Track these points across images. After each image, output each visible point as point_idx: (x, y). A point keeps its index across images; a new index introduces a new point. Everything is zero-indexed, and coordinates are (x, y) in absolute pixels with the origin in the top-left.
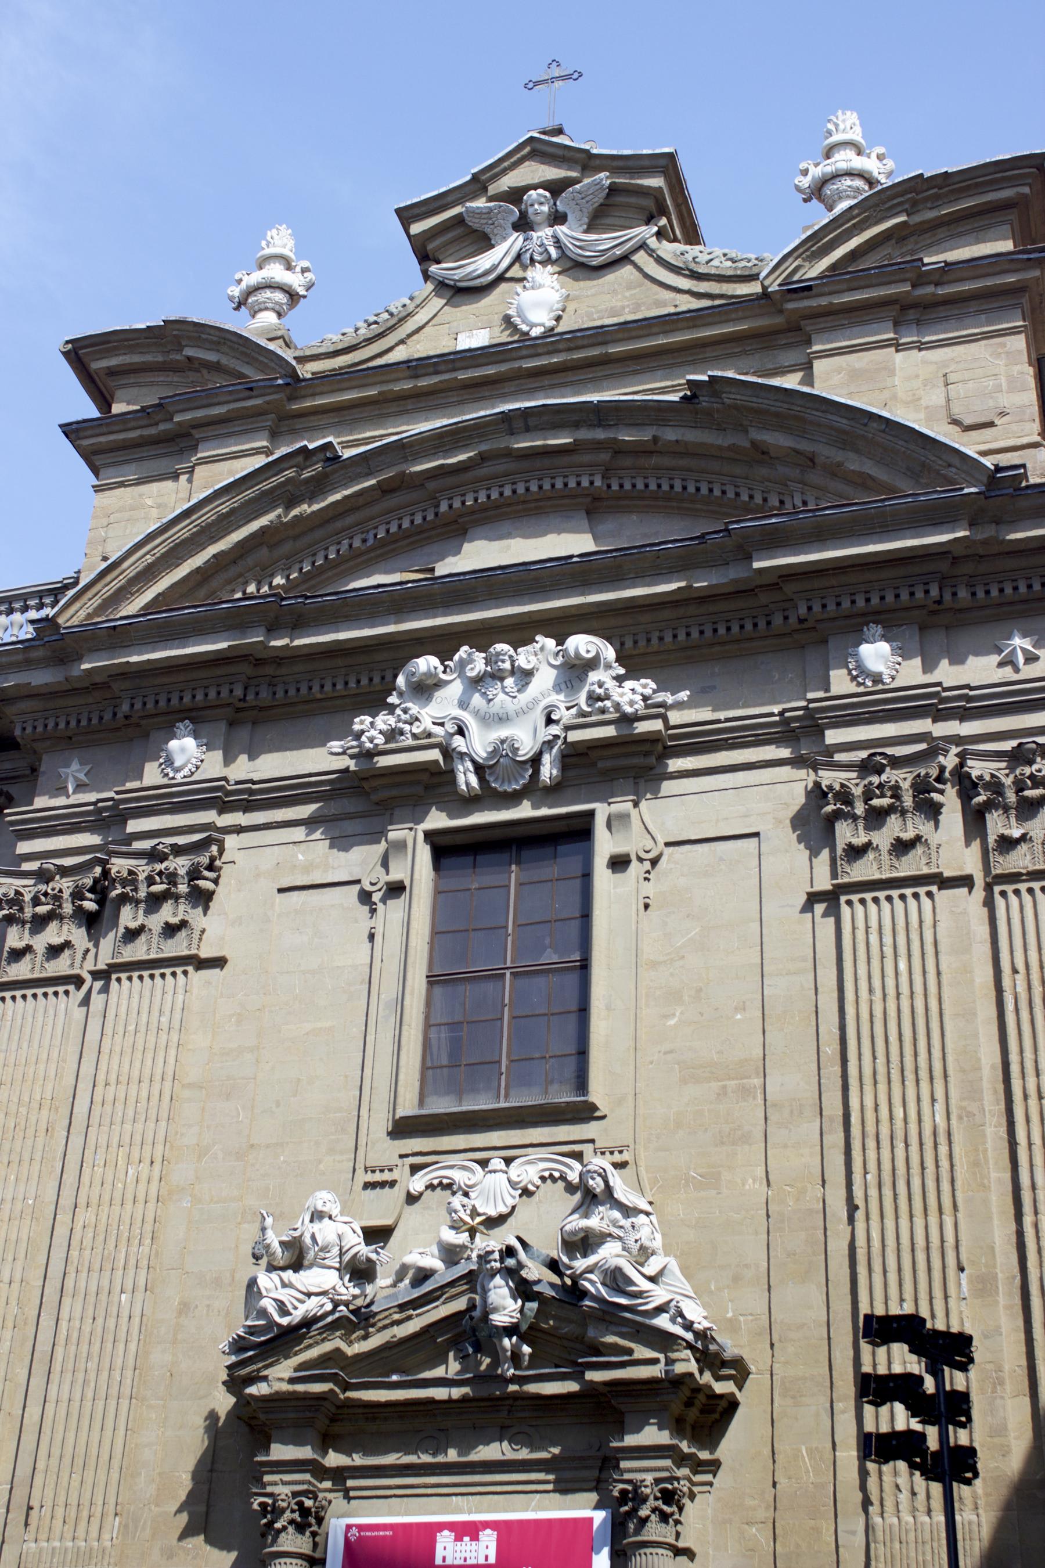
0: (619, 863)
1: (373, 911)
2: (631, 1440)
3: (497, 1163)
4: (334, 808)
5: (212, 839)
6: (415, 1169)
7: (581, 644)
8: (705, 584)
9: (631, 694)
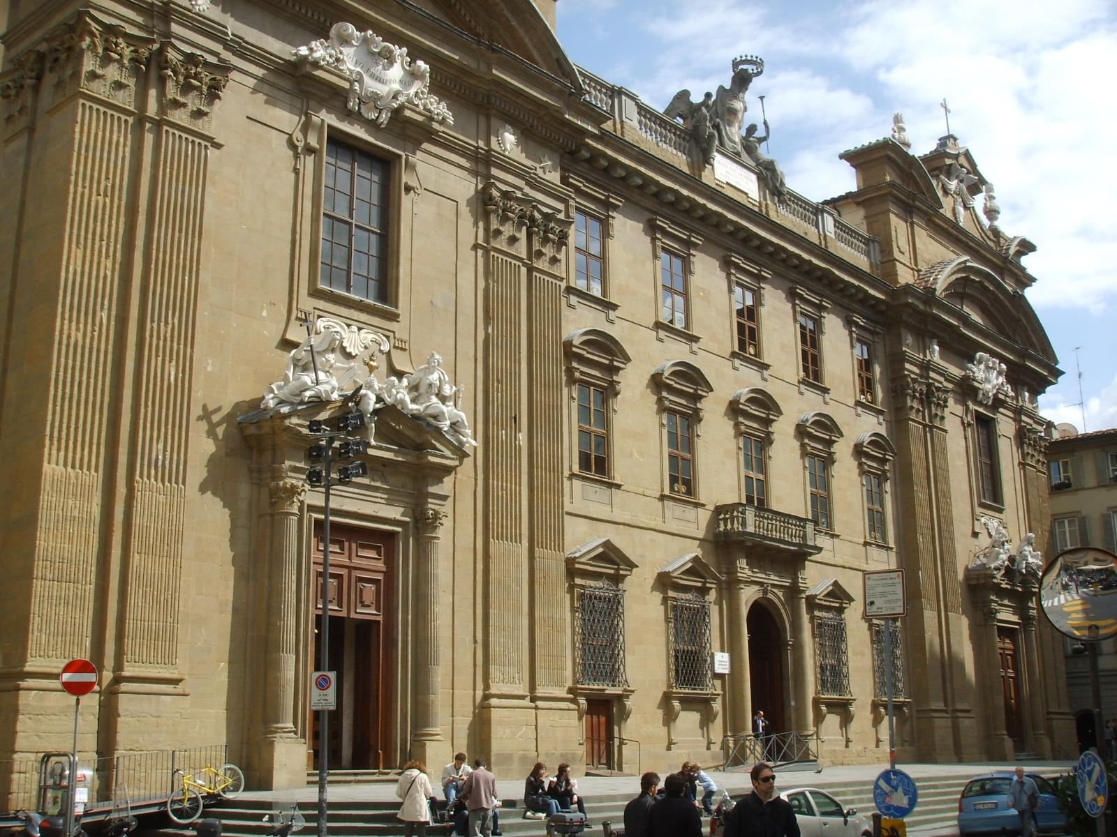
0: (408, 189)
1: (296, 156)
2: (432, 489)
3: (354, 328)
4: (271, 78)
5: (225, 68)
6: (319, 317)
7: (422, 65)
8: (457, 58)
9: (440, 108)
